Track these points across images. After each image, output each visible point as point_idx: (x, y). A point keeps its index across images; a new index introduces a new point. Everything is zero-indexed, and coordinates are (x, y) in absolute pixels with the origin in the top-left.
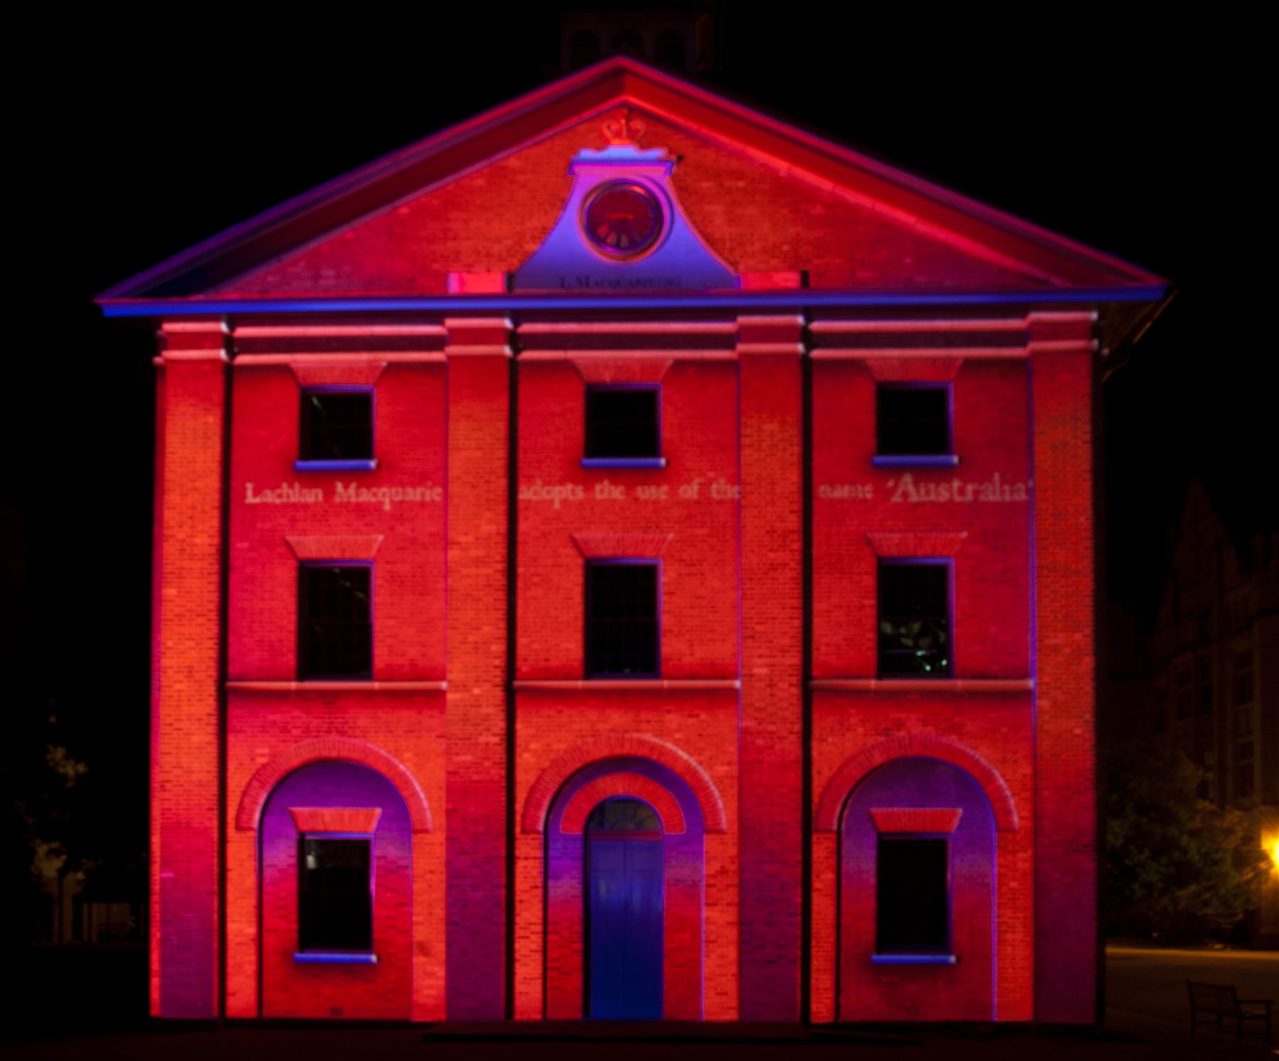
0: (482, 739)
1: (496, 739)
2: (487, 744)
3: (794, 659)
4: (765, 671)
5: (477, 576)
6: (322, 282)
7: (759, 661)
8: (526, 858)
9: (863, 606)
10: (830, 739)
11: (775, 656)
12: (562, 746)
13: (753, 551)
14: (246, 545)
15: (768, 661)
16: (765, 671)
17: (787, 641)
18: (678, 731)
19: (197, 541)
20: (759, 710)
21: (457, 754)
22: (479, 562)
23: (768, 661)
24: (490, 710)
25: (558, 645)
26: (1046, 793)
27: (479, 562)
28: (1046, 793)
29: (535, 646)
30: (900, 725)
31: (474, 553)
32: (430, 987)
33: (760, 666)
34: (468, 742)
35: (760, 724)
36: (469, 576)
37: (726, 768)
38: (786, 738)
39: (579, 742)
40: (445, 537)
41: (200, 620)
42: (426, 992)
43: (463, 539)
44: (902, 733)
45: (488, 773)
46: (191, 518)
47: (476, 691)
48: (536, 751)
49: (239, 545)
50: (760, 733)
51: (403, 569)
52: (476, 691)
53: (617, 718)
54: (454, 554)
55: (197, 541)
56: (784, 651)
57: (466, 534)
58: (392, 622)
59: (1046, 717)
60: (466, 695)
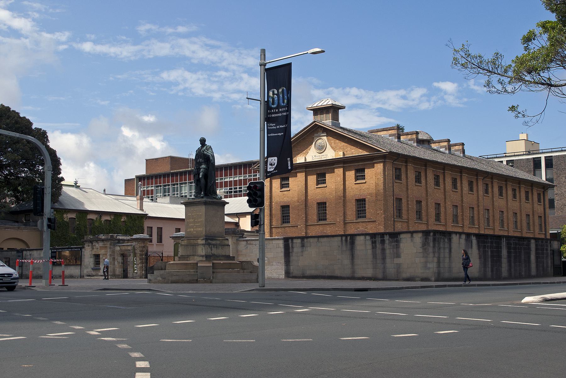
0: (302, 233)
1: (304, 233)
3: (342, 218)
7: (338, 218)
12: (314, 234)
17: (341, 215)
22: (302, 205)
27: (302, 205)
51: (293, 206)
53: (321, 228)
58: (292, 215)
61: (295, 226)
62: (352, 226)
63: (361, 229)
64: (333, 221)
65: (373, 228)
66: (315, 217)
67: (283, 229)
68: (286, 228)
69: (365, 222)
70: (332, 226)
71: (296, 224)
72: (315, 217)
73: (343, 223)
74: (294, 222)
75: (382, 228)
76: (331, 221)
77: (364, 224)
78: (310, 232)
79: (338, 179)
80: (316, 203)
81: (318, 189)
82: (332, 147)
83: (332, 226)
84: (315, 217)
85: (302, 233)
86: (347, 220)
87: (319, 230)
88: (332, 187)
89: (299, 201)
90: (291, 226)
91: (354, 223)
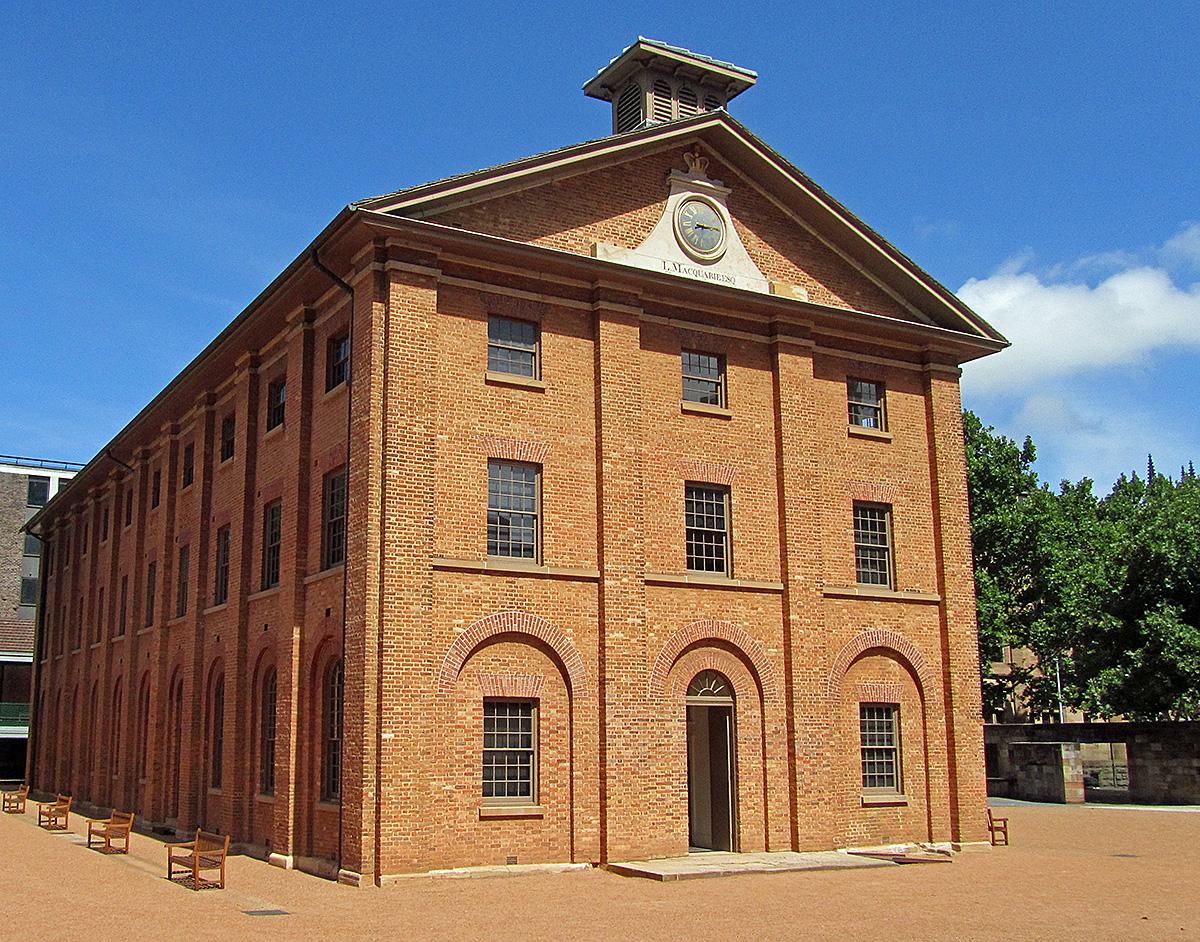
0: (630, 620)
1: (639, 621)
4: (802, 578)
5: (623, 485)
7: (799, 570)
8: (652, 721)
14: (445, 437)
16: (802, 578)
18: (747, 621)
21: (612, 632)
24: (634, 596)
29: (654, 546)
33: (799, 574)
35: (801, 617)
36: (618, 486)
43: (612, 454)
44: (873, 629)
45: (634, 649)
46: (410, 409)
47: (625, 580)
48: (658, 631)
51: (563, 473)
52: (625, 580)
53: (708, 602)
55: (415, 429)
57: (615, 451)
60: (618, 582)
62: (845, 611)
65: (925, 629)
66: (677, 547)
72: (677, 547)
73: (818, 593)
75: (968, 633)
76: (753, 579)
79: (796, 397)
81: (689, 419)
82: (752, 256)
85: (630, 620)
87: (697, 613)
88: (757, 426)
89: (612, 454)
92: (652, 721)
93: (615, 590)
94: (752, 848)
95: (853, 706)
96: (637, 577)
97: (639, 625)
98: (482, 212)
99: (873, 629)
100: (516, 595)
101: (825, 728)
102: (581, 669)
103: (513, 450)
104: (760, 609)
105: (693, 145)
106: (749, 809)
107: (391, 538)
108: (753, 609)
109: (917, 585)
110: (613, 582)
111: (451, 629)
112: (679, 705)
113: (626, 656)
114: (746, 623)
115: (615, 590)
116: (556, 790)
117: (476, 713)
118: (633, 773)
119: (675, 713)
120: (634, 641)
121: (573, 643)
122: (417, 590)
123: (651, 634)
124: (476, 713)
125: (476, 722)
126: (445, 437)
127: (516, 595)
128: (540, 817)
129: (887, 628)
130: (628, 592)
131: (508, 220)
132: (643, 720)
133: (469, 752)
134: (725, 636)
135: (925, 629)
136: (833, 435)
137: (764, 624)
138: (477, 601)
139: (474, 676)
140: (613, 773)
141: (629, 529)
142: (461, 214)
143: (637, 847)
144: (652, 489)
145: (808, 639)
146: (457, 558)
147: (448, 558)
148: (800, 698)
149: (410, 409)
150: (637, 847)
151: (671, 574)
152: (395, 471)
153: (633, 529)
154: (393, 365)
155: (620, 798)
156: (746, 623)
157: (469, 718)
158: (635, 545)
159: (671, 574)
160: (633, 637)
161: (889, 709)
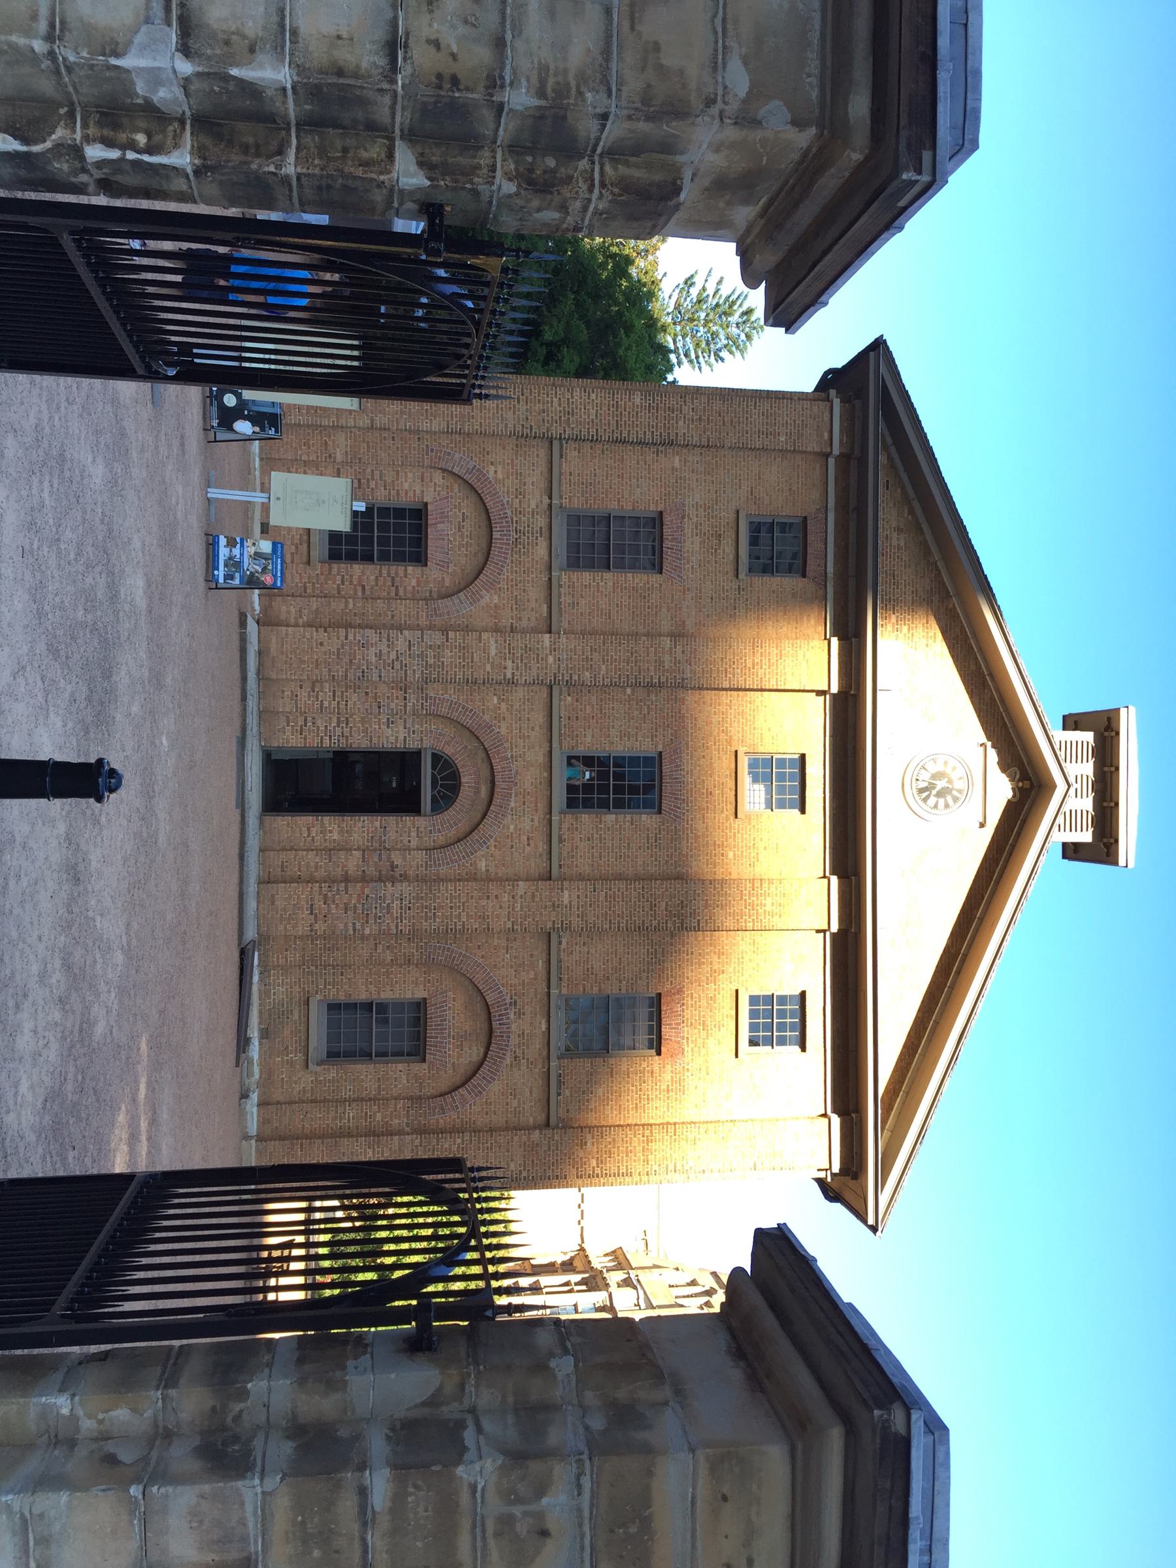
1: (509, 676)
2: (505, 668)
4: (566, 902)
6: (895, 535)
9: (620, 982)
10: (508, 956)
11: (578, 908)
12: (504, 731)
13: (667, 890)
14: (677, 464)
15: (574, 903)
16: (566, 902)
18: (516, 828)
19: (681, 423)
20: (533, 896)
21: (496, 641)
23: (574, 903)
25: (589, 726)
26: (459, 1141)
27: (659, 663)
28: (459, 1141)
30: (520, 1014)
31: (667, 658)
32: (289, 612)
33: (570, 896)
34: (507, 651)
36: (648, 654)
37: (484, 869)
38: (509, 920)
39: (507, 745)
40: (682, 635)
41: (613, 422)
42: (284, 608)
44: (512, 1016)
45: (480, 667)
46: (700, 419)
47: (551, 659)
49: (677, 458)
50: (513, 897)
52: (551, 659)
53: (530, 778)
54: (667, 642)
55: (681, 423)
56: (582, 916)
57: (683, 652)
59: (524, 1138)
60: (548, 652)
61: (550, 607)
62: (532, 975)
63: (514, 1026)
64: (565, 854)
66: (589, 739)
67: (541, 521)
68: (543, 545)
69: (545, 1053)
70: (536, 847)
71: (560, 610)
72: (589, 739)
73: (550, 925)
74: (569, 600)
76: (561, 841)
77: (537, 1044)
78: (516, 707)
80: (660, 748)
83: (536, 847)
84: (589, 743)
85: (509, 664)
86: (564, 941)
90: (550, 579)
91: (544, 984)
92: (405, 698)
93: (539, 646)
94: (265, 832)
95: (422, 987)
96: (555, 674)
97: (505, 675)
98: (906, 515)
99: (512, 1016)
100: (528, 538)
101: (397, 927)
102: (459, 608)
103: (673, 540)
104: (528, 848)
105: (1029, 779)
106: (309, 829)
107: (575, 394)
108: (528, 839)
109: (567, 1092)
110: (547, 643)
111: (492, 464)
112: (422, 740)
113: (472, 657)
114: (512, 827)
115: (539, 646)
116: (334, 583)
117: (411, 494)
118: (351, 661)
119: (414, 732)
120: (488, 668)
121: (483, 602)
122: (527, 419)
123: (495, 700)
124: (411, 494)
125: (402, 494)
126: (677, 464)
127: (528, 538)
128: (308, 563)
129: (514, 1040)
130: (538, 662)
131: (902, 543)
132: (406, 676)
133: (373, 484)
134: (497, 800)
135: (515, 1103)
136: (733, 966)
137: (512, 853)
138: (520, 493)
139: (448, 493)
140: (351, 637)
141: (604, 667)
142: (899, 491)
143: (273, 662)
144: (648, 707)
145: (498, 907)
146: (560, 586)
147: (561, 465)
148: (431, 891)
149: (700, 419)
150: (273, 662)
151: (560, 730)
152: (639, 400)
153: (603, 672)
154: (740, 402)
155: (325, 643)
156: (512, 827)
157: (406, 486)
158: (587, 674)
159: (560, 730)
160: (492, 668)
161: (417, 1050)
